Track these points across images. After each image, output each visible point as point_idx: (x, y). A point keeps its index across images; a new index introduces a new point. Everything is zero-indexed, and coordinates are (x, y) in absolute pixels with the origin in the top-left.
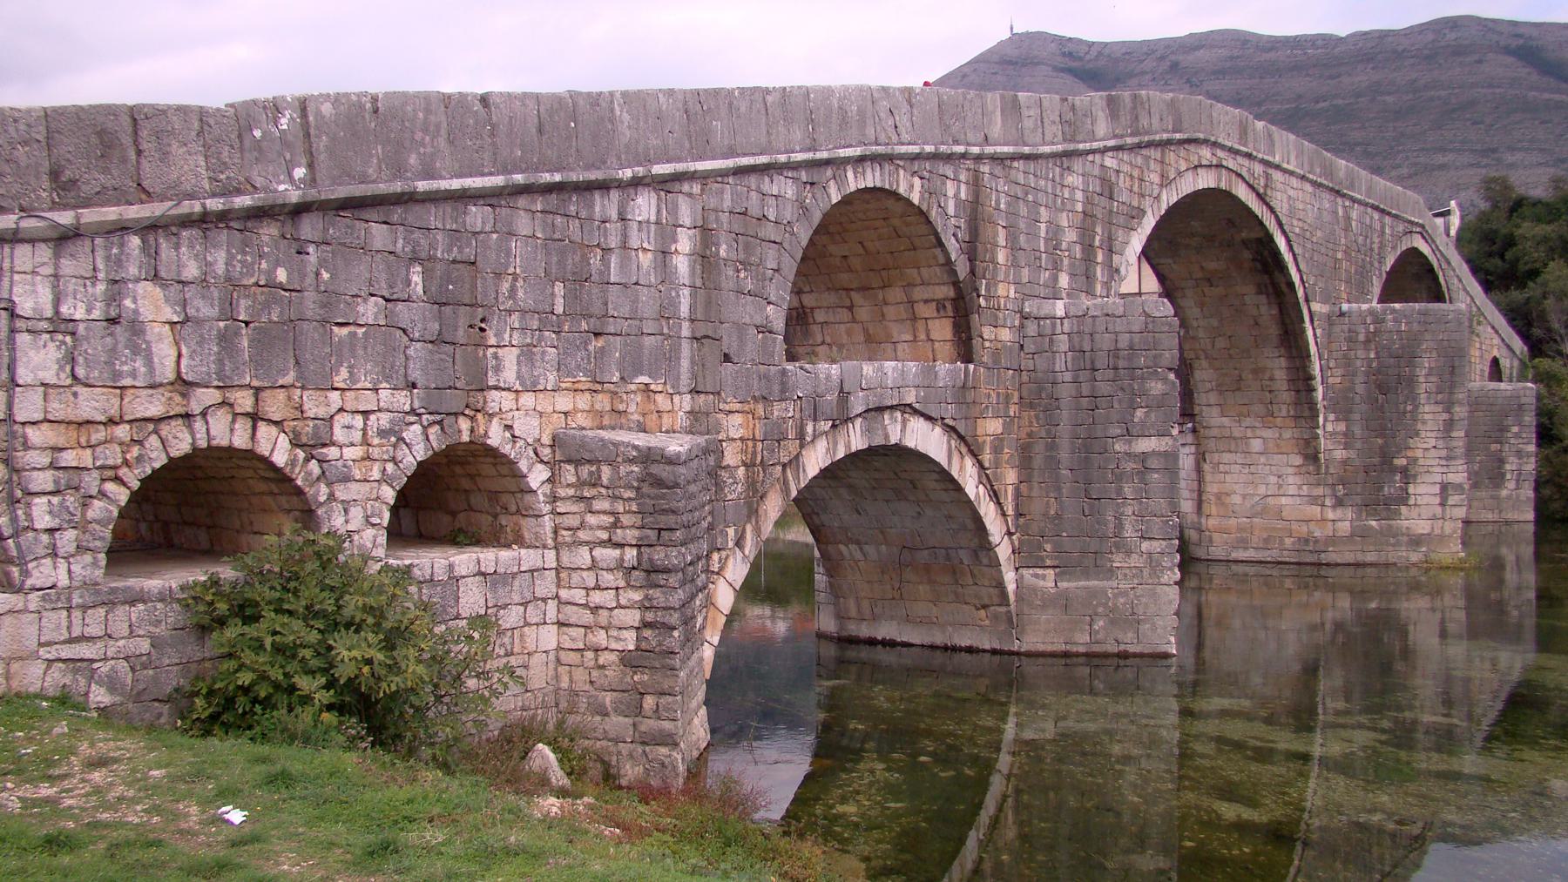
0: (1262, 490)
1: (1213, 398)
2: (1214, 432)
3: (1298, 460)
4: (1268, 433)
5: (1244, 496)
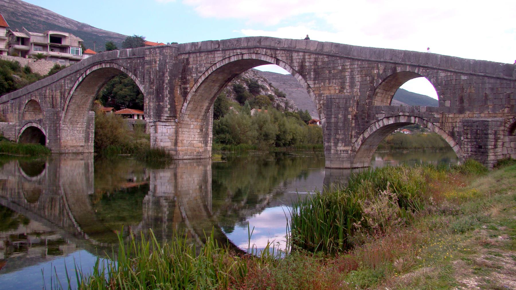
0: (190, 139)
1: (188, 113)
2: (185, 122)
3: (199, 131)
4: (195, 123)
5: (187, 141)
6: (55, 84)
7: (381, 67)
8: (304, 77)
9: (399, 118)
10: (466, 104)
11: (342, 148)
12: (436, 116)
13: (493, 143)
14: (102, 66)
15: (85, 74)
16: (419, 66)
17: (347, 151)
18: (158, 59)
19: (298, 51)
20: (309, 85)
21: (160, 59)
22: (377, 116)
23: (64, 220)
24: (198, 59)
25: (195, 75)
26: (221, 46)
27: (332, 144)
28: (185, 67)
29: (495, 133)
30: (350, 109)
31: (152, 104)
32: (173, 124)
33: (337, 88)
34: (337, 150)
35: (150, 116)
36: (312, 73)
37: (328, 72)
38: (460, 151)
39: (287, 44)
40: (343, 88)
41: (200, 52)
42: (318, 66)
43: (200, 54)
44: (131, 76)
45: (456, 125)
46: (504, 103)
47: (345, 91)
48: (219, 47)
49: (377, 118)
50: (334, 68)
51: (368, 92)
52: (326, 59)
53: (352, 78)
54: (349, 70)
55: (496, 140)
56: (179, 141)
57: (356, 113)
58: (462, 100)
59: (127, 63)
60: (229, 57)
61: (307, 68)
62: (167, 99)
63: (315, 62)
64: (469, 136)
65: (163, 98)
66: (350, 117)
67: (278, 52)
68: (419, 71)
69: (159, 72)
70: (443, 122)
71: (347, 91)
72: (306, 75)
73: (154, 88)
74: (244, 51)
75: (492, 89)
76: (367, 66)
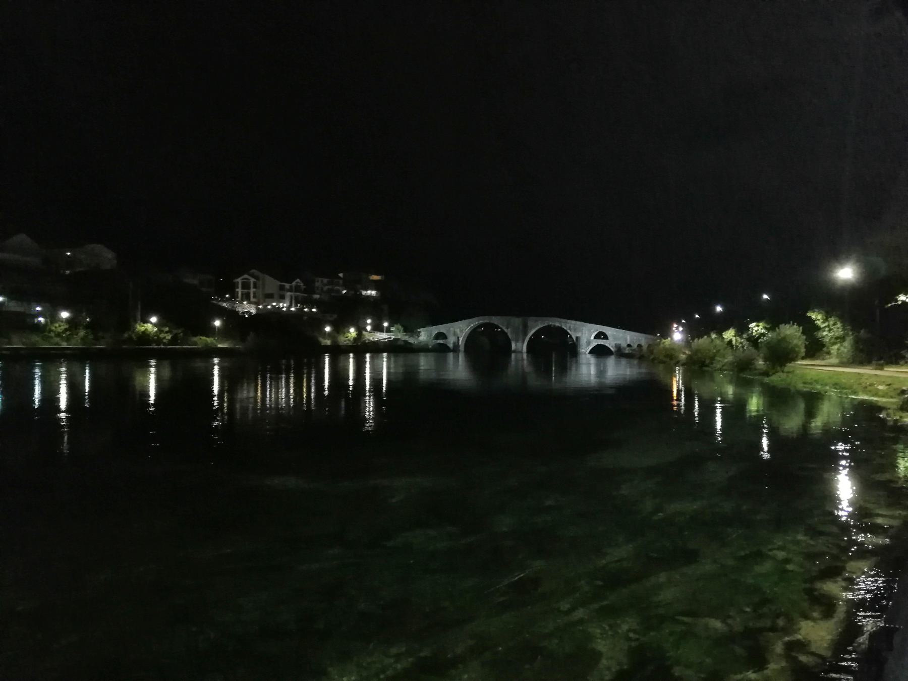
40: (582, 334)
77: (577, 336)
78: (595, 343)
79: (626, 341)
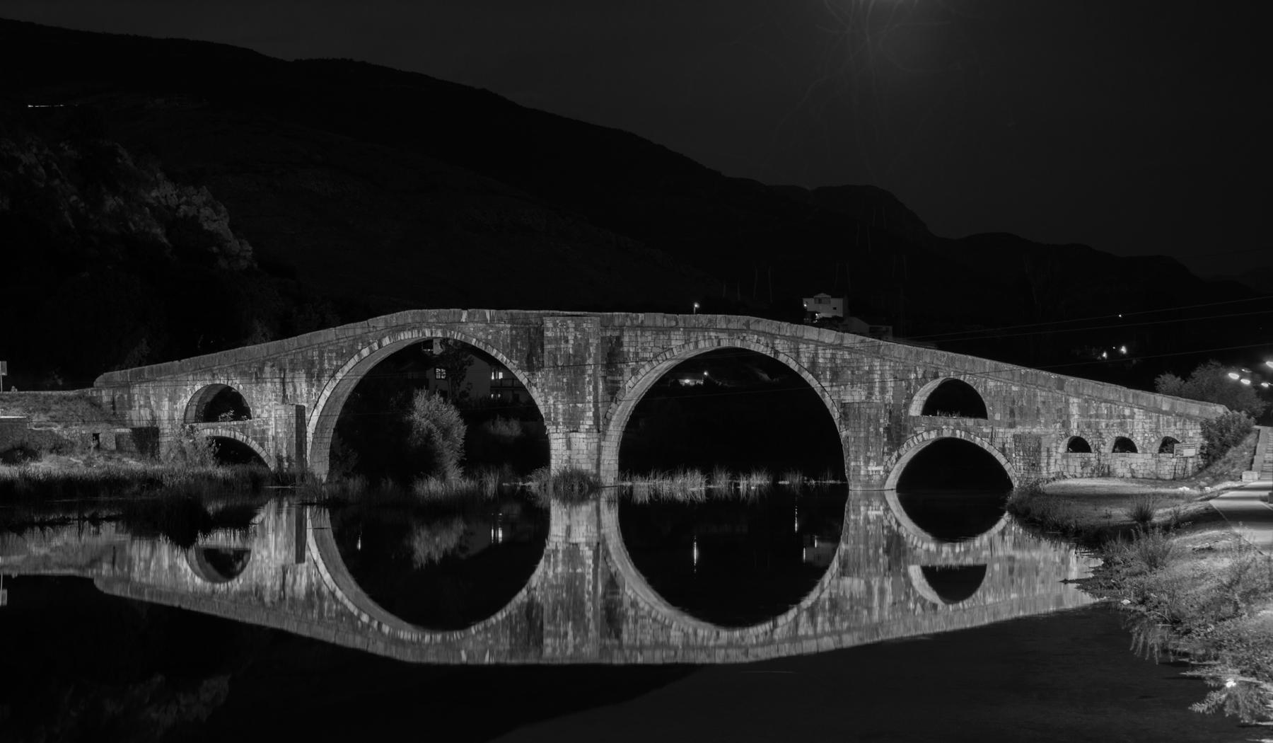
6: (289, 357)
7: (920, 372)
8: (817, 377)
9: (942, 432)
10: (1017, 419)
11: (875, 468)
12: (985, 430)
13: (1046, 461)
14: (424, 334)
15: (380, 346)
16: (965, 374)
17: (879, 471)
18: (571, 338)
19: (808, 342)
20: (823, 387)
21: (575, 337)
22: (915, 429)
23: (321, 607)
24: (639, 339)
25: (632, 364)
26: (681, 324)
27: (862, 464)
28: (614, 349)
29: (1048, 450)
30: (882, 421)
31: (560, 406)
32: (595, 435)
33: (863, 393)
34: (868, 471)
35: (557, 424)
36: (828, 373)
37: (849, 372)
38: (1012, 469)
39: (791, 332)
40: (870, 394)
41: (642, 327)
42: (837, 364)
43: (642, 333)
44: (497, 355)
45: (1007, 441)
46: (1056, 417)
47: (874, 398)
48: (677, 323)
49: (915, 432)
50: (858, 369)
51: (904, 401)
52: (847, 356)
53: (883, 382)
54: (879, 372)
55: (1049, 457)
56: (601, 462)
57: (888, 425)
58: (1012, 413)
59: (488, 335)
60: (697, 343)
61: (821, 365)
62: (590, 398)
63: (833, 358)
64: (1021, 453)
65: (584, 397)
66: (881, 430)
67: (777, 342)
68: (965, 378)
69: (575, 356)
70: (992, 438)
71: (877, 397)
72: (819, 375)
73: (565, 380)
74: (722, 335)
75: (1044, 403)
76: (902, 368)
77: (848, 399)
78: (922, 437)
79: (1066, 425)
